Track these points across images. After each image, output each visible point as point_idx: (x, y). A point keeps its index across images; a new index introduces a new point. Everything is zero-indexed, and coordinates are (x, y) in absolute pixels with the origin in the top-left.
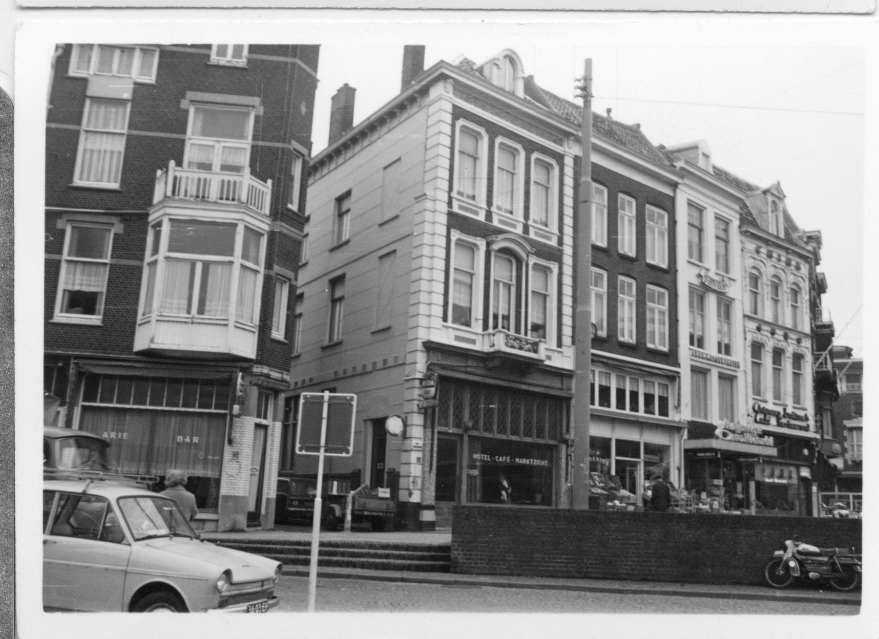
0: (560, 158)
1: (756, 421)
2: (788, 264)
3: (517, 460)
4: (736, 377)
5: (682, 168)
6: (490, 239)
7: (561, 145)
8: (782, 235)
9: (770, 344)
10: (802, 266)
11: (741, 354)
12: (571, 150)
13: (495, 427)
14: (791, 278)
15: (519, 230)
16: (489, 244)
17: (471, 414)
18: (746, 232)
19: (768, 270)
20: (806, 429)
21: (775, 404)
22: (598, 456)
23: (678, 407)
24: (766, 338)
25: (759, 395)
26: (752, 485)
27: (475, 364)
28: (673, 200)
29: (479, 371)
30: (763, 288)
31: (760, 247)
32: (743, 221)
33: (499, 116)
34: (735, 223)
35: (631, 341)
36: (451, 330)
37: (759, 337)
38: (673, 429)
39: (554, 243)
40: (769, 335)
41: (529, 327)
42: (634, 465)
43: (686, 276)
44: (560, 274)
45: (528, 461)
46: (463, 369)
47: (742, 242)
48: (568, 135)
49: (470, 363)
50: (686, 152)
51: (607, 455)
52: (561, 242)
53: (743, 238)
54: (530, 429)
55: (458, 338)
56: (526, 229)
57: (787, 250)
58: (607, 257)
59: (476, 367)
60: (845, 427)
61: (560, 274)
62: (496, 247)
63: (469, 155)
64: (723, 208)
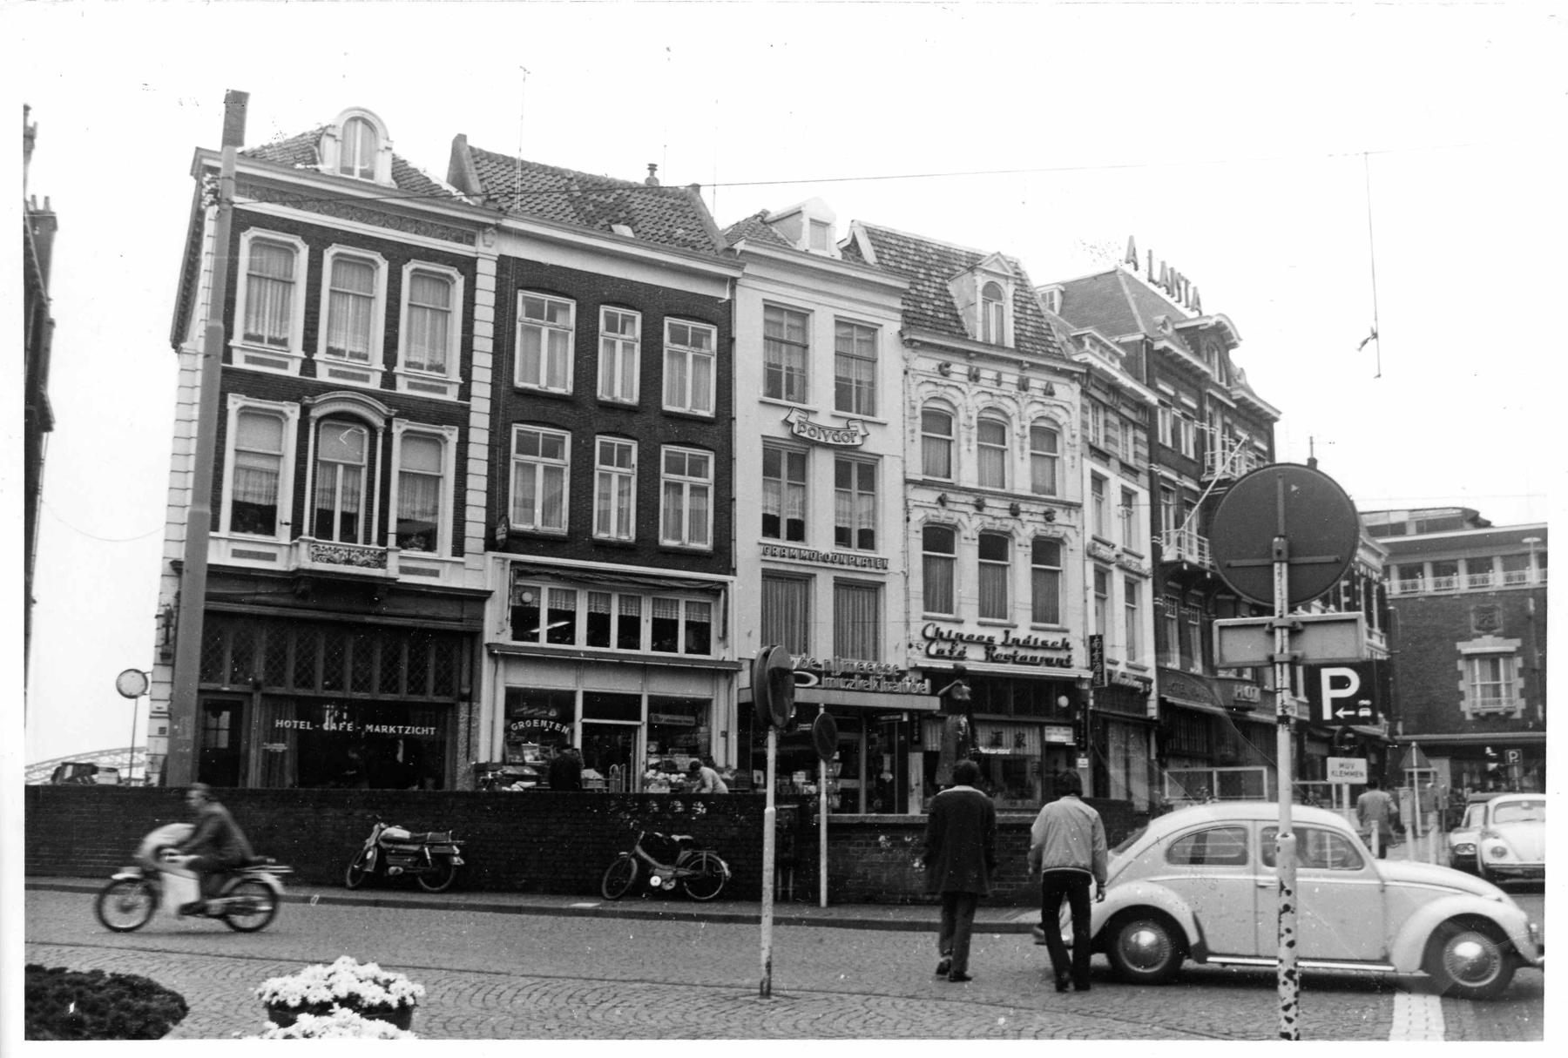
0: (468, 266)
1: (929, 655)
2: (1023, 386)
3: (370, 727)
4: (883, 584)
5: (742, 252)
6: (307, 400)
7: (472, 244)
8: (1010, 343)
9: (970, 527)
10: (1057, 388)
11: (899, 546)
12: (487, 253)
13: (404, 684)
14: (1034, 411)
15: (375, 384)
16: (305, 411)
17: (268, 663)
18: (911, 341)
19: (969, 404)
20: (1066, 663)
21: (981, 624)
22: (556, 720)
23: (724, 637)
24: (964, 518)
25: (951, 612)
26: (916, 761)
27: (275, 589)
28: (729, 306)
29: (282, 600)
30: (958, 432)
31: (948, 365)
32: (911, 320)
33: (334, 215)
34: (891, 327)
35: (624, 537)
36: (223, 543)
37: (942, 515)
38: (725, 672)
39: (452, 396)
40: (972, 510)
41: (393, 526)
42: (635, 728)
43: (755, 423)
44: (463, 443)
45: (392, 729)
46: (247, 598)
47: (906, 360)
48: (483, 226)
49: (262, 589)
50: (787, 221)
51: (568, 718)
52: (465, 392)
53: (908, 352)
54: (396, 682)
55: (237, 554)
56: (389, 379)
57: (1019, 363)
58: (581, 412)
59: (282, 595)
60: (1459, 655)
61: (463, 443)
62: (316, 413)
63: (274, 280)
64: (847, 304)
